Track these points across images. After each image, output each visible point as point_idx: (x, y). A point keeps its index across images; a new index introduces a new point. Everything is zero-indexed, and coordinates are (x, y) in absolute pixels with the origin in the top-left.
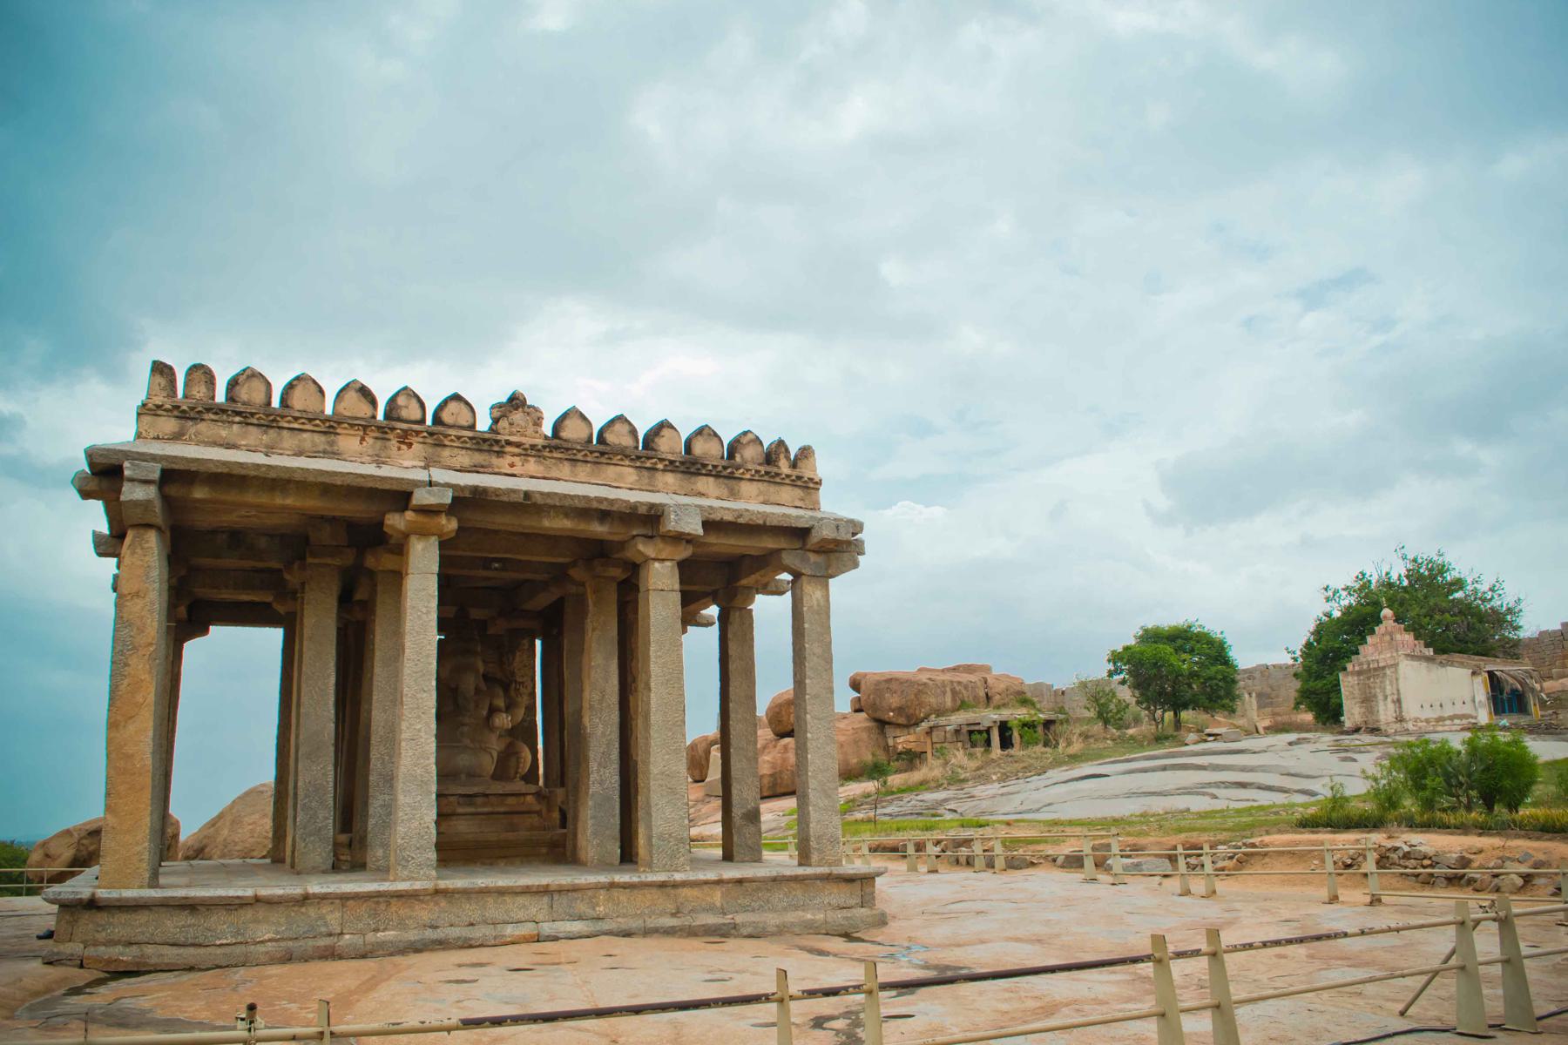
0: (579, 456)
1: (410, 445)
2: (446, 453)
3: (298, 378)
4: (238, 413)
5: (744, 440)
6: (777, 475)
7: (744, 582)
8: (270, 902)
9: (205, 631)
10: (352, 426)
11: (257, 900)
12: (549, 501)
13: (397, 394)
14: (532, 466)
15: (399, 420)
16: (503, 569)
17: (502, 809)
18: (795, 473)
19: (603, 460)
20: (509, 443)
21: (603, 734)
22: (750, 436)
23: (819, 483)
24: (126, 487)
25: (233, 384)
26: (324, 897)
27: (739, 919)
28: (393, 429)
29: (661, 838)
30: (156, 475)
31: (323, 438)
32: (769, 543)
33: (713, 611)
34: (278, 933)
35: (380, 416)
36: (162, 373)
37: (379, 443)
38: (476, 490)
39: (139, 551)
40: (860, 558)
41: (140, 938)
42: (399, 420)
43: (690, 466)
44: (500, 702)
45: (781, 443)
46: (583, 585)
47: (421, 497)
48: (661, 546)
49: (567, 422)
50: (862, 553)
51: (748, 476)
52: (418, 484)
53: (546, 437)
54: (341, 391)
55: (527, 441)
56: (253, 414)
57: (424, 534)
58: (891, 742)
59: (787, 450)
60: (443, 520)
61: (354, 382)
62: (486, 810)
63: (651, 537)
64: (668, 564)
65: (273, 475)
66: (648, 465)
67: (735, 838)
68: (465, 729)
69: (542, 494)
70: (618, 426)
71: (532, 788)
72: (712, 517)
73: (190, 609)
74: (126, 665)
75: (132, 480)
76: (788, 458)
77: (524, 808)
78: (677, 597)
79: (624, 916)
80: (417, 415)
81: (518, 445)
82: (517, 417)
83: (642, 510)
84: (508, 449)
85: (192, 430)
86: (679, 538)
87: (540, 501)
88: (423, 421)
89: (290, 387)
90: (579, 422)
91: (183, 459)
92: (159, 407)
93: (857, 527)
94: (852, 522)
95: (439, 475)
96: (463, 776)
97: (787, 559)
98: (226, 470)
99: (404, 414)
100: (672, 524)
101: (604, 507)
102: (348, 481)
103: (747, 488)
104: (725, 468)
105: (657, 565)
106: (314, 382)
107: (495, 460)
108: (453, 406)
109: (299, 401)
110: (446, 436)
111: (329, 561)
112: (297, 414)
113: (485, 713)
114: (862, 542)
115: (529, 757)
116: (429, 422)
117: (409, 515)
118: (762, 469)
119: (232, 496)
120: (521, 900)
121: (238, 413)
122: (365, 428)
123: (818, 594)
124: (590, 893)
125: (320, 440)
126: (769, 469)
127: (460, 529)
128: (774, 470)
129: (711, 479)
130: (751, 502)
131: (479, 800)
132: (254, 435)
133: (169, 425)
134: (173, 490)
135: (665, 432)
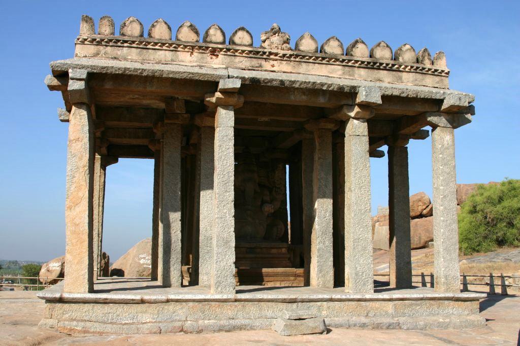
2: (237, 59)
4: (126, 42)
5: (404, 49)
6: (424, 69)
7: (403, 132)
8: (150, 302)
9: (116, 161)
11: (142, 302)
14: (285, 66)
15: (211, 42)
18: (434, 68)
19: (324, 62)
20: (271, 54)
24: (71, 82)
26: (177, 301)
27: (402, 320)
28: (207, 48)
30: (84, 76)
31: (171, 53)
32: (419, 108)
33: (385, 148)
34: (154, 319)
36: (87, 22)
39: (78, 117)
41: (86, 318)
42: (211, 42)
45: (425, 50)
46: (312, 133)
50: (473, 114)
52: (221, 77)
54: (180, 27)
57: (226, 107)
59: (429, 54)
65: (145, 74)
66: (350, 64)
69: (291, 81)
71: (285, 245)
72: (387, 93)
73: (109, 149)
74: (75, 177)
75: (72, 79)
79: (337, 316)
81: (276, 54)
82: (276, 39)
83: (346, 90)
84: (272, 57)
85: (103, 52)
92: (86, 40)
95: (232, 72)
99: (214, 39)
102: (185, 76)
103: (405, 76)
105: (356, 122)
108: (240, 34)
110: (236, 51)
118: (416, 65)
120: (281, 305)
121: (126, 42)
122: (193, 48)
124: (319, 304)
126: (418, 65)
127: (245, 103)
128: (421, 66)
129: (385, 72)
130: (408, 84)
132: (133, 54)
133: (92, 49)
135: (360, 46)
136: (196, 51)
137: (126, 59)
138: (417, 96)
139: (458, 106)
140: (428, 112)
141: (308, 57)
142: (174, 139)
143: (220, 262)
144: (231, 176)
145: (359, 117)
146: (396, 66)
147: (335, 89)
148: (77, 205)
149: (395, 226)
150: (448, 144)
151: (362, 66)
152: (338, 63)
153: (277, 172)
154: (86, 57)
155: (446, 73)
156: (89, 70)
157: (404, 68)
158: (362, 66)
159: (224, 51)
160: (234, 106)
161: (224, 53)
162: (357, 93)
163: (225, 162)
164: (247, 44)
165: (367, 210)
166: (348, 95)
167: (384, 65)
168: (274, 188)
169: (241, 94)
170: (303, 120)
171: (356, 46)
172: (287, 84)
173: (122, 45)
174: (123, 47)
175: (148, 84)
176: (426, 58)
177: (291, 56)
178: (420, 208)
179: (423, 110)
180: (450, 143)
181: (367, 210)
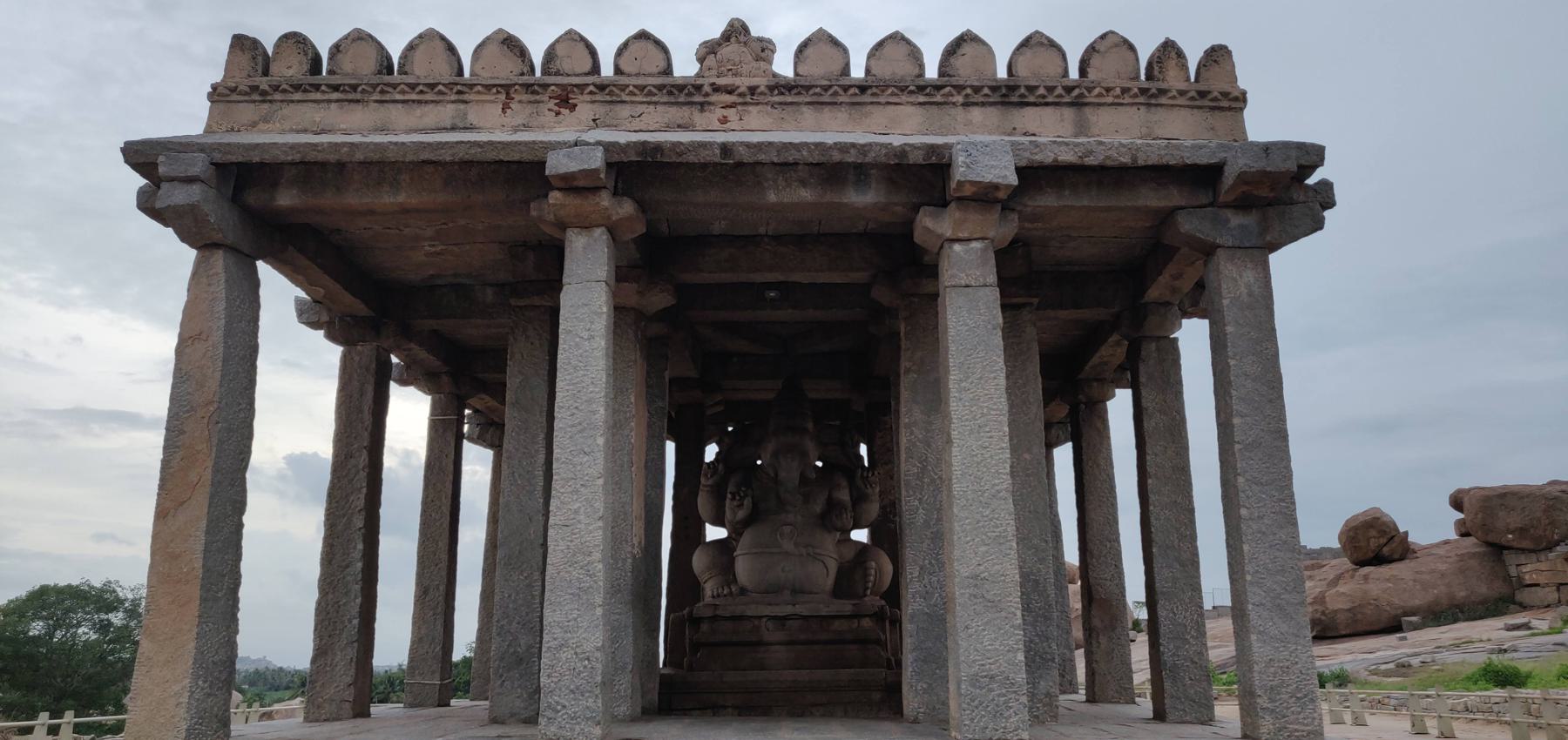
0: (826, 98)
1: (573, 107)
2: (624, 111)
3: (420, 36)
4: (336, 88)
5: (1101, 47)
6: (1162, 92)
7: (1153, 293)
10: (488, 87)
12: (762, 157)
13: (557, 41)
19: (866, 98)
20: (717, 89)
21: (927, 524)
22: (1110, 40)
23: (1242, 98)
25: (336, 49)
28: (545, 86)
29: (974, 681)
35: (538, 73)
37: (529, 109)
39: (204, 280)
40: (1327, 214)
42: (558, 73)
43: (1010, 95)
44: (844, 495)
47: (558, 164)
48: (957, 214)
49: (809, 51)
51: (1110, 100)
53: (775, 75)
55: (743, 83)
56: (354, 88)
57: (587, 227)
58: (1513, 571)
59: (1180, 55)
60: (605, 200)
61: (501, 30)
62: (802, 637)
63: (945, 205)
64: (976, 245)
65: (359, 156)
66: (938, 98)
67: (1167, 685)
68: (787, 529)
69: (748, 145)
70: (887, 49)
74: (182, 432)
75: (172, 180)
76: (1185, 67)
78: (995, 294)
80: (588, 66)
81: (730, 91)
82: (727, 51)
83: (916, 158)
84: (714, 98)
86: (984, 197)
87: (746, 156)
88: (596, 69)
89: (411, 48)
90: (829, 49)
91: (239, 146)
92: (233, 90)
93: (1312, 156)
94: (1302, 147)
97: (1189, 225)
98: (297, 157)
99: (566, 66)
100: (962, 171)
102: (461, 154)
104: (1069, 89)
105: (957, 247)
106: (443, 38)
107: (699, 119)
109: (422, 70)
110: (623, 88)
111: (537, 301)
112: (410, 80)
113: (818, 507)
114: (1326, 186)
115: (889, 568)
116: (607, 70)
117: (555, 197)
119: (328, 200)
121: (336, 88)
122: (507, 88)
123: (1249, 276)
125: (446, 113)
129: (1049, 110)
133: (247, 112)
134: (253, 198)
135: (966, 48)
136: (517, 97)
138: (1134, 159)
139: (1264, 174)
140: (1182, 208)
141: (818, 90)
144: (594, 412)
145: (965, 235)
146: (1076, 92)
147: (883, 159)
148: (182, 504)
150: (1250, 294)
151: (978, 98)
152: (904, 98)
155: (1236, 99)
156: (218, 157)
157: (1100, 95)
158: (978, 98)
159: (591, 93)
160: (612, 231)
161: (588, 98)
162: (949, 165)
164: (656, 70)
166: (926, 177)
167: (1042, 91)
169: (624, 194)
170: (859, 277)
171: (960, 52)
173: (326, 97)
174: (329, 101)
176: (1172, 63)
177: (771, 88)
178: (1373, 544)
179: (1163, 204)
180: (1256, 289)
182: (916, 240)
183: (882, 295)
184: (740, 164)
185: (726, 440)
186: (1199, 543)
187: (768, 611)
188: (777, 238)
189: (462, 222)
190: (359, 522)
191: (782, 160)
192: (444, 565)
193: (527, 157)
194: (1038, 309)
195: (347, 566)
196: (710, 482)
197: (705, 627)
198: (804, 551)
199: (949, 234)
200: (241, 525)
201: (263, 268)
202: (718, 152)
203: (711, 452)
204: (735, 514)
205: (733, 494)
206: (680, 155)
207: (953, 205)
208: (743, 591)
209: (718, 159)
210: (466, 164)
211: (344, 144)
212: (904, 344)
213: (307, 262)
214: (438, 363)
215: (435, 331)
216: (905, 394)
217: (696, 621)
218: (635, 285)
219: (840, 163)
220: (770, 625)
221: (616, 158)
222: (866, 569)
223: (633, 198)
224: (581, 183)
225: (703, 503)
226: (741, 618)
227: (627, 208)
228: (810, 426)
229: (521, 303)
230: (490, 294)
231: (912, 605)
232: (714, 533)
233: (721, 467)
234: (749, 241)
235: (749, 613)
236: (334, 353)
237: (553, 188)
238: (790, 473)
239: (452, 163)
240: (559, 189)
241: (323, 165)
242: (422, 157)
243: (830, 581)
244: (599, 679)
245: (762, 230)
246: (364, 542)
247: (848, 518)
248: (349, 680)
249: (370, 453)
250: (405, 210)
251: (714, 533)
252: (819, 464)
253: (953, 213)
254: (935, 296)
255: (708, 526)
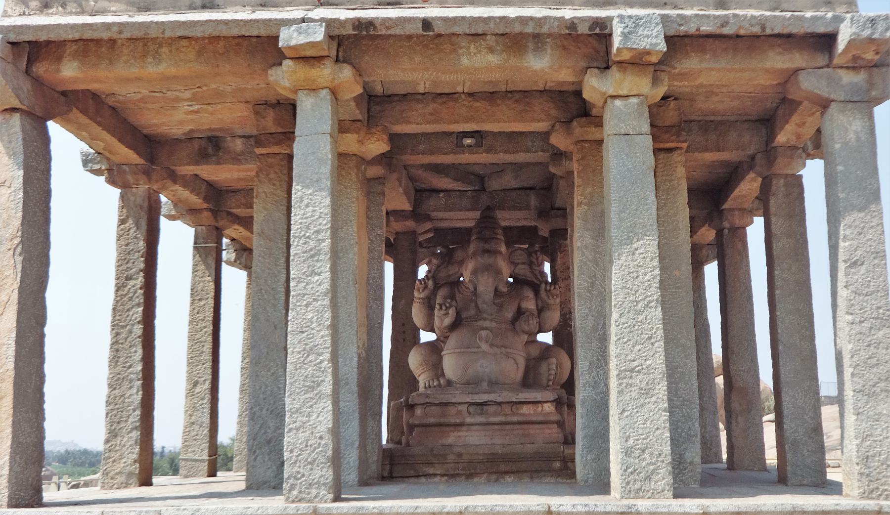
12: (457, 29)
16: (479, 145)
17: (515, 419)
38: (359, 24)
44: (530, 305)
57: (314, 90)
63: (608, 67)
64: (634, 100)
65: (126, 35)
69: (445, 20)
77: (540, 418)
83: (583, 29)
91: (28, 27)
96: (485, 385)
98: (77, 36)
101: (529, 29)
102: (210, 31)
105: (618, 102)
111: (276, 149)
113: (509, 314)
131: (492, 409)
134: (41, 69)
137: (103, 12)
142: (274, 185)
143: (297, 429)
144: (323, 241)
145: (624, 92)
147: (556, 30)
149: (780, 348)
153: (560, 255)
154: (24, 14)
160: (334, 92)
163: (311, 208)
165: (650, 302)
168: (543, 286)
169: (345, 61)
170: (541, 126)
172: (439, 28)
175: (150, 60)
181: (650, 302)
182: (584, 96)
183: (559, 140)
184: (439, 36)
185: (435, 261)
186: (817, 342)
187: (469, 399)
188: (470, 95)
189: (213, 86)
190: (138, 330)
191: (473, 31)
192: (209, 364)
193: (263, 32)
194: (687, 151)
195: (130, 367)
196: (422, 296)
197: (419, 411)
198: (497, 350)
199: (611, 92)
200: (43, 336)
201: (54, 128)
202: (420, 25)
203: (422, 271)
204: (442, 321)
205: (441, 305)
206: (388, 28)
207: (614, 68)
208: (449, 383)
209: (420, 32)
210: (214, 39)
211: (114, 24)
212: (577, 181)
213: (88, 121)
214: (200, 201)
215: (196, 175)
216: (578, 223)
217: (411, 407)
218: (356, 136)
219: (521, 33)
220: (471, 409)
221: (336, 32)
222: (549, 365)
223: (351, 64)
224: (309, 53)
225: (417, 315)
226: (447, 404)
227: (346, 72)
228: (503, 249)
229: (264, 151)
230: (238, 145)
231: (582, 393)
232: (426, 337)
233: (430, 283)
234: (449, 96)
235: (454, 401)
236: (116, 192)
237: (285, 58)
238: (486, 286)
239: (203, 38)
240: (292, 59)
241: (98, 42)
242: (179, 34)
243: (520, 375)
244: (330, 453)
245: (459, 89)
246: (144, 347)
247: (533, 323)
248: (135, 456)
249: (145, 277)
250: (166, 78)
251: (426, 337)
252: (511, 280)
253: (615, 73)
254: (600, 142)
255: (422, 332)
